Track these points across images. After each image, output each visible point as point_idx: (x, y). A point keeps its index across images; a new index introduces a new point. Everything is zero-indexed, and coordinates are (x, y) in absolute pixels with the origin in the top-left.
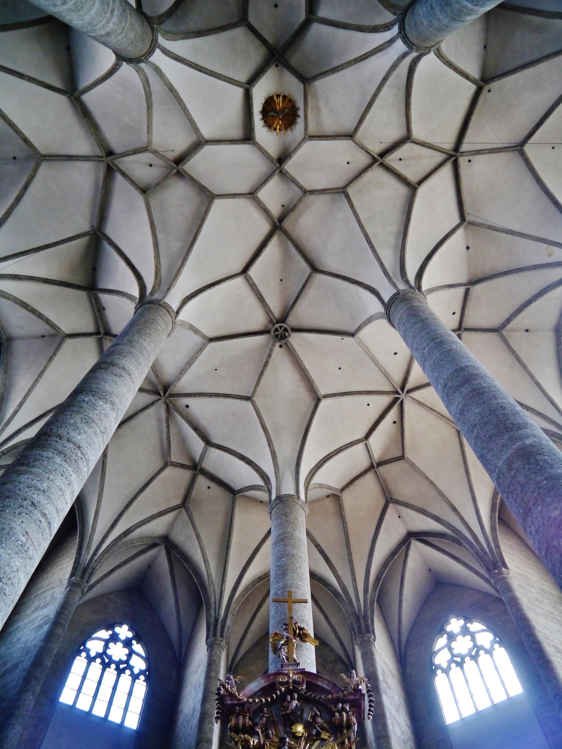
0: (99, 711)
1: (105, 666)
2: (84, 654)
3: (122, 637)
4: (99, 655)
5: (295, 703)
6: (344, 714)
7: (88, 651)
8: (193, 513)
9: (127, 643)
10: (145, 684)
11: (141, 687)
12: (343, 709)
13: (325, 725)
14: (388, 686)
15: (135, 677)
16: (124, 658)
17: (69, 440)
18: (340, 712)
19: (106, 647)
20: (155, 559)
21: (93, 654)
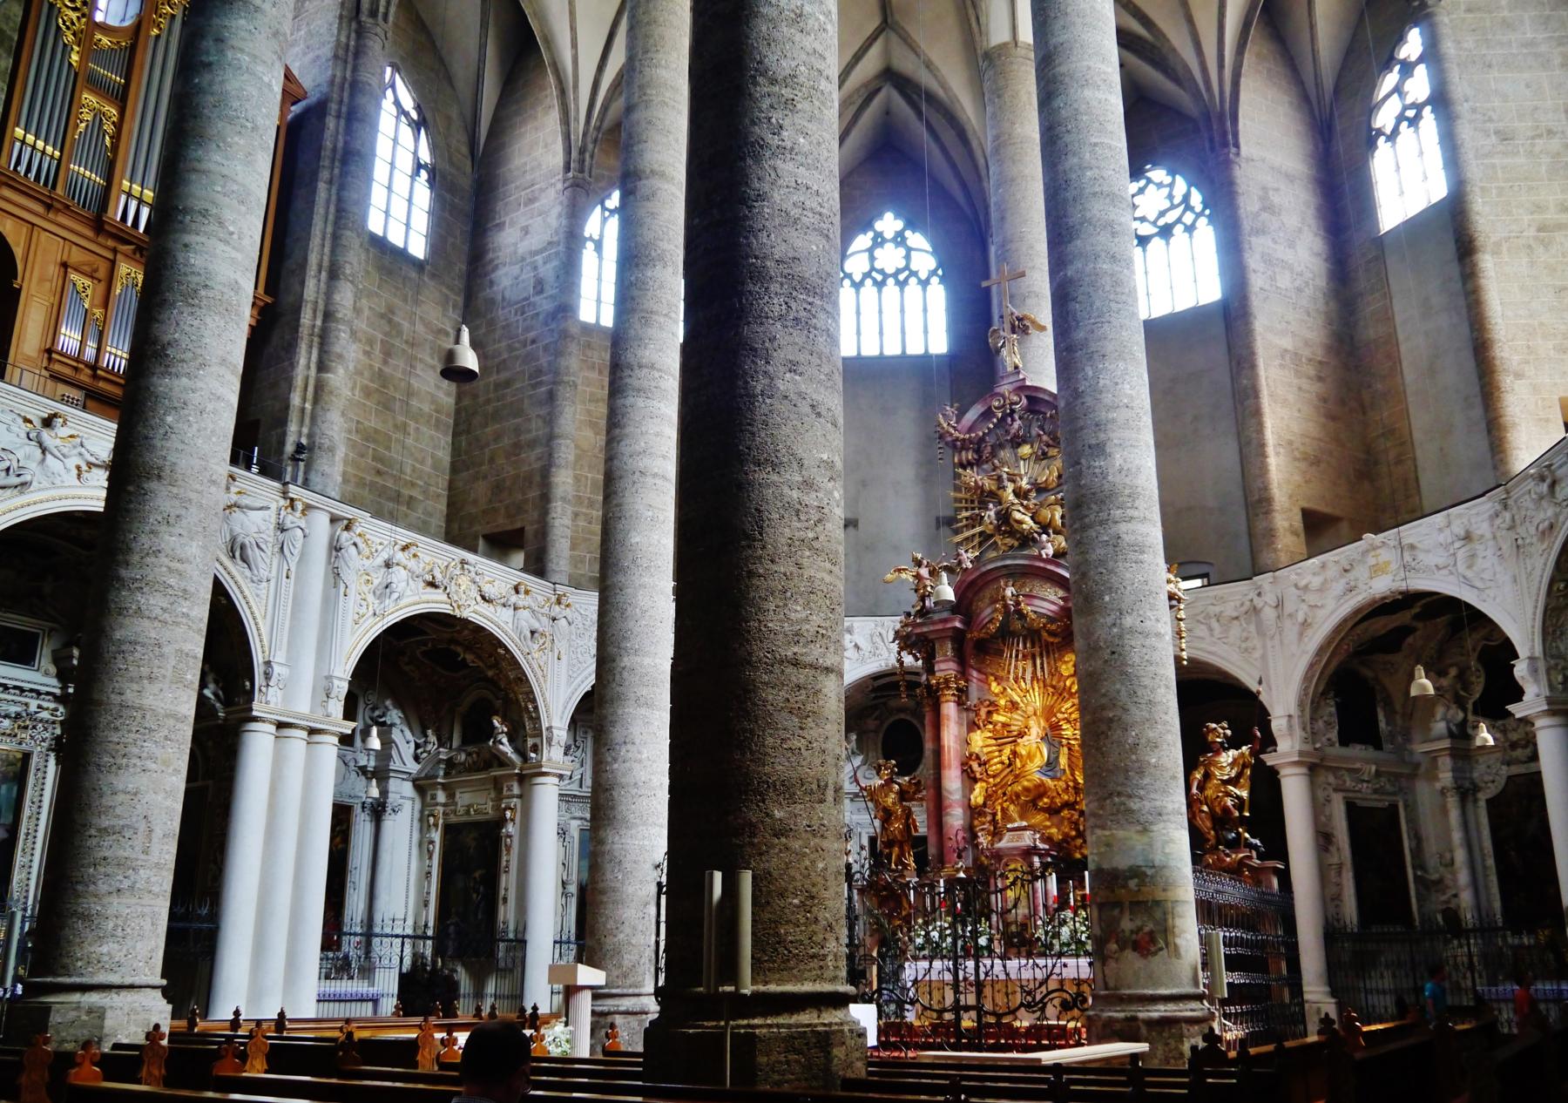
0: (893, 350)
1: (880, 285)
2: (847, 282)
3: (889, 235)
4: (867, 275)
5: (1017, 423)
7: (849, 276)
8: (908, 28)
9: (899, 239)
10: (941, 287)
11: (938, 294)
14: (1273, 213)
15: (925, 283)
16: (902, 264)
17: (640, 367)
19: (872, 259)
20: (887, 112)
21: (857, 278)
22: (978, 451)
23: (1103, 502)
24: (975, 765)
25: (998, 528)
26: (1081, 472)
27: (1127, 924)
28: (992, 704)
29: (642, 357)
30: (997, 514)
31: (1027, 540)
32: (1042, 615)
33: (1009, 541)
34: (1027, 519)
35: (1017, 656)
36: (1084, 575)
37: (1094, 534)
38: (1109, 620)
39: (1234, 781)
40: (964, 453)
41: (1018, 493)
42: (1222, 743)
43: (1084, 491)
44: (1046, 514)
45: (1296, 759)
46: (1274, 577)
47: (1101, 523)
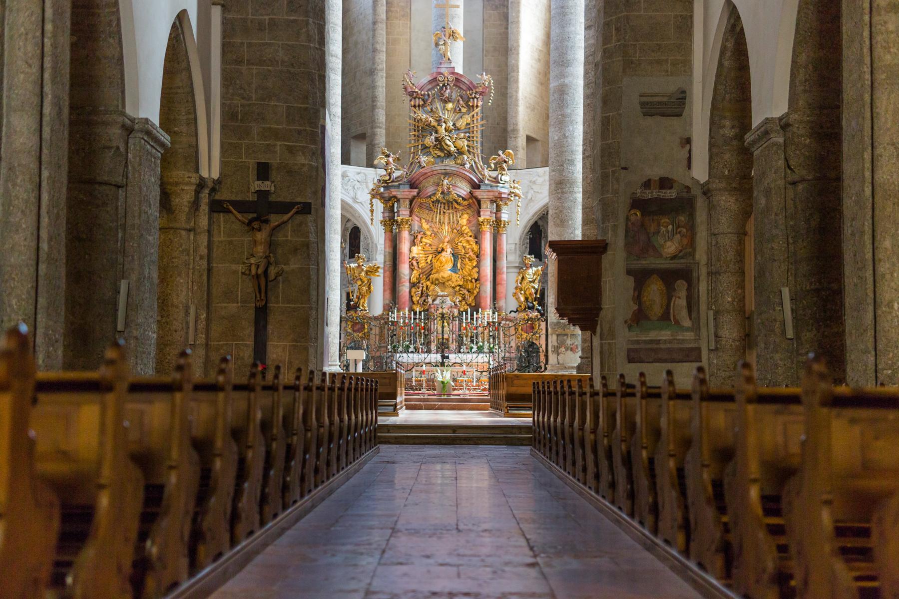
5: (448, 91)
6: (475, 100)
12: (475, 97)
13: (464, 105)
17: (332, 56)
18: (473, 98)
22: (425, 101)
23: (571, 184)
24: (415, 263)
25: (435, 145)
26: (563, 170)
27: (569, 342)
28: (424, 234)
29: (333, 50)
30: (437, 139)
31: (449, 155)
32: (459, 196)
33: (439, 153)
34: (452, 145)
35: (440, 212)
36: (561, 211)
37: (567, 196)
38: (570, 231)
39: (533, 281)
40: (417, 99)
42: (531, 265)
43: (563, 178)
45: (517, 265)
46: (516, 173)
47: (570, 192)
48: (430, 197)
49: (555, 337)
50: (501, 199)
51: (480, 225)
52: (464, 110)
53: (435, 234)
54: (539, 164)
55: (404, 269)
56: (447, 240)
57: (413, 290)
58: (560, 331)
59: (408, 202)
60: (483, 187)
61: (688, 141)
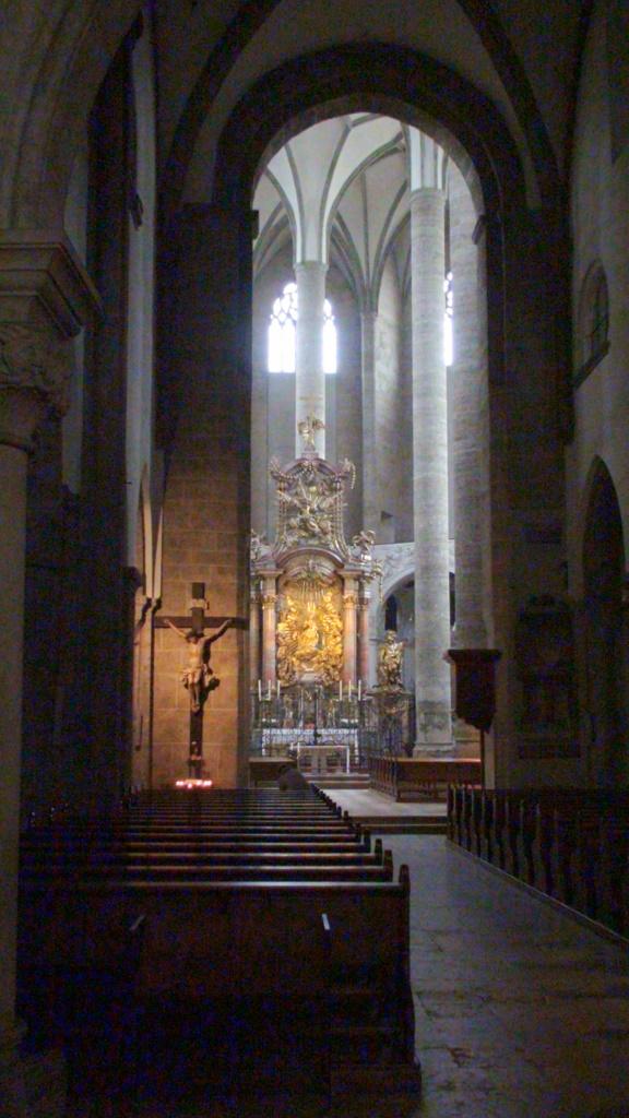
25: (300, 528)
28: (290, 611)
30: (302, 520)
31: (313, 535)
32: (323, 574)
33: (304, 534)
39: (395, 657)
41: (312, 511)
44: (323, 524)
48: (296, 575)
49: (422, 716)
50: (364, 577)
51: (343, 602)
52: (327, 493)
53: (300, 612)
54: (393, 540)
55: (270, 645)
56: (311, 617)
57: (279, 666)
58: (427, 710)
59: (274, 581)
60: (346, 567)
61: (565, 565)
